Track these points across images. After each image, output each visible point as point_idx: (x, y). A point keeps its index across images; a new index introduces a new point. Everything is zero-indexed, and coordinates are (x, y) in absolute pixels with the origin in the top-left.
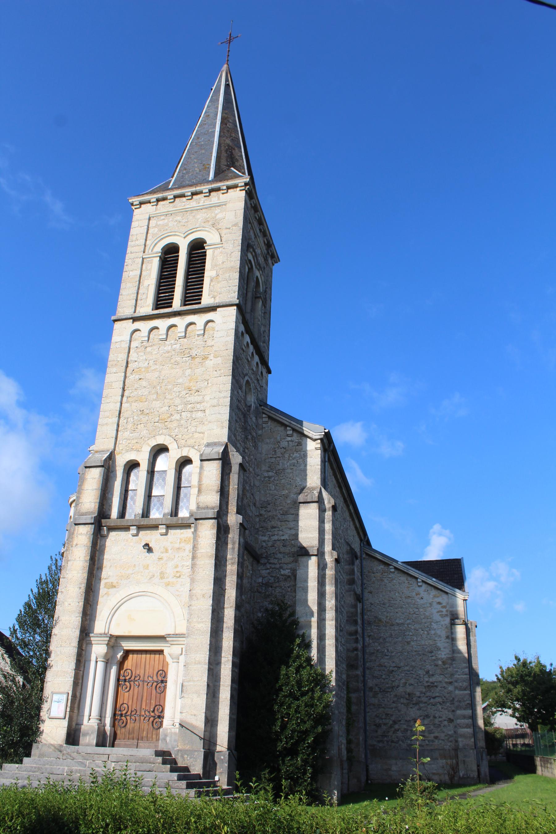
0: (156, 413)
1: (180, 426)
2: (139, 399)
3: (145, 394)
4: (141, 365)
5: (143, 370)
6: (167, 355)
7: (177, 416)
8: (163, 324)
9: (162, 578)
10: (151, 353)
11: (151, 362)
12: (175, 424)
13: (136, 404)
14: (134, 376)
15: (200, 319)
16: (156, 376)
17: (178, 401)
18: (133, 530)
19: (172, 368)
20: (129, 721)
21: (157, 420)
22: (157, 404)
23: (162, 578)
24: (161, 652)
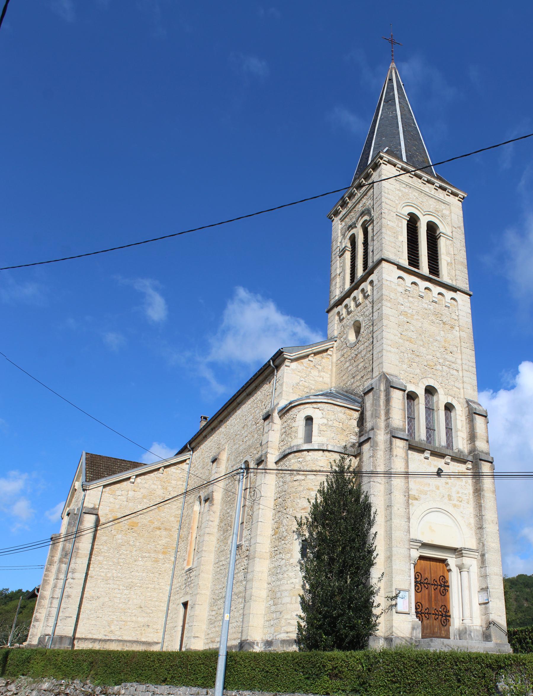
0: (424, 357)
1: (442, 376)
2: (410, 340)
3: (414, 337)
4: (406, 310)
5: (409, 315)
6: (426, 311)
7: (439, 367)
8: (410, 279)
9: (450, 500)
10: (411, 302)
11: (414, 313)
12: (440, 374)
13: (408, 343)
14: (402, 317)
15: (437, 289)
16: (420, 326)
17: (438, 355)
18: (427, 454)
19: (430, 325)
20: (424, 618)
21: (426, 364)
22: (423, 350)
23: (450, 500)
24: (443, 561)
